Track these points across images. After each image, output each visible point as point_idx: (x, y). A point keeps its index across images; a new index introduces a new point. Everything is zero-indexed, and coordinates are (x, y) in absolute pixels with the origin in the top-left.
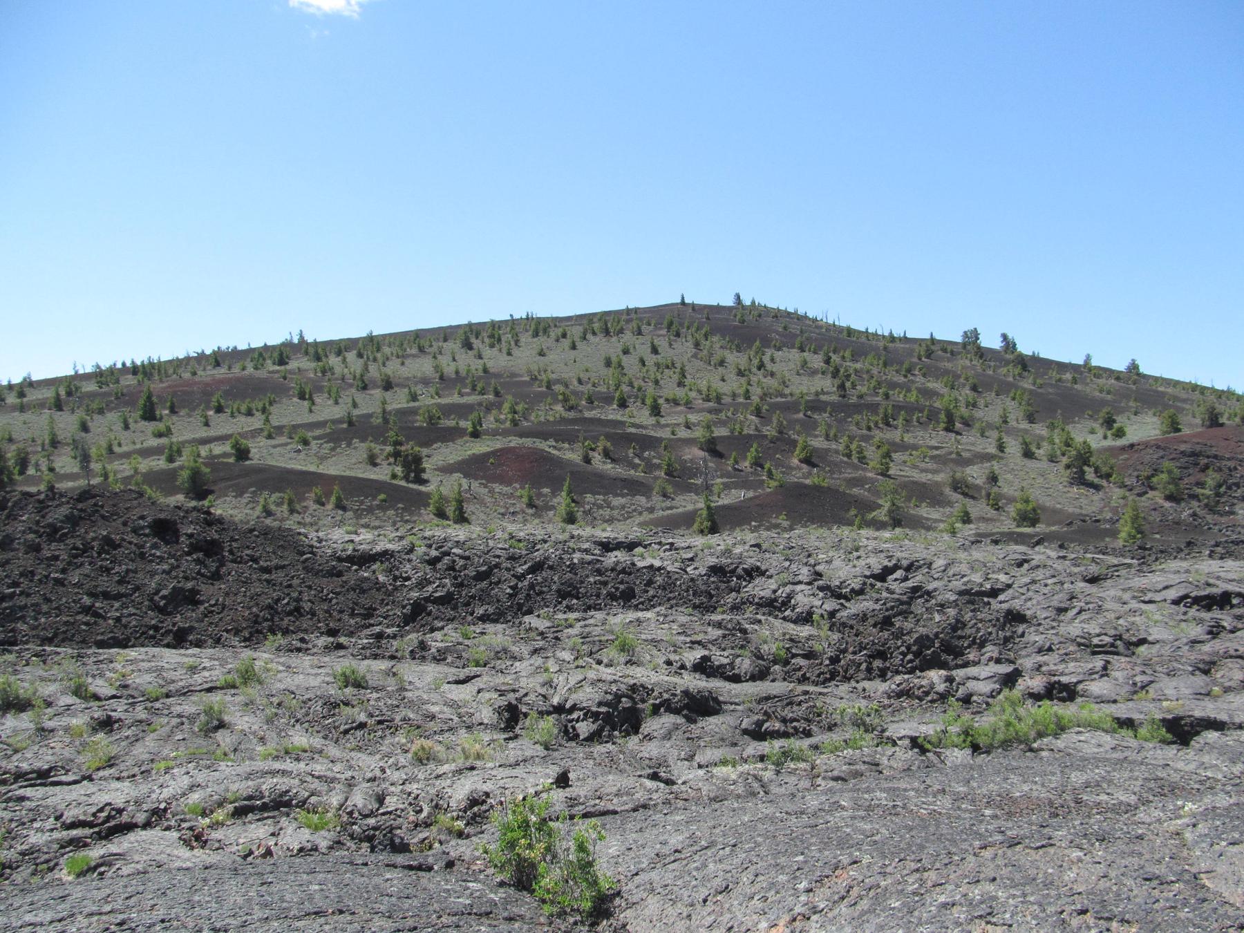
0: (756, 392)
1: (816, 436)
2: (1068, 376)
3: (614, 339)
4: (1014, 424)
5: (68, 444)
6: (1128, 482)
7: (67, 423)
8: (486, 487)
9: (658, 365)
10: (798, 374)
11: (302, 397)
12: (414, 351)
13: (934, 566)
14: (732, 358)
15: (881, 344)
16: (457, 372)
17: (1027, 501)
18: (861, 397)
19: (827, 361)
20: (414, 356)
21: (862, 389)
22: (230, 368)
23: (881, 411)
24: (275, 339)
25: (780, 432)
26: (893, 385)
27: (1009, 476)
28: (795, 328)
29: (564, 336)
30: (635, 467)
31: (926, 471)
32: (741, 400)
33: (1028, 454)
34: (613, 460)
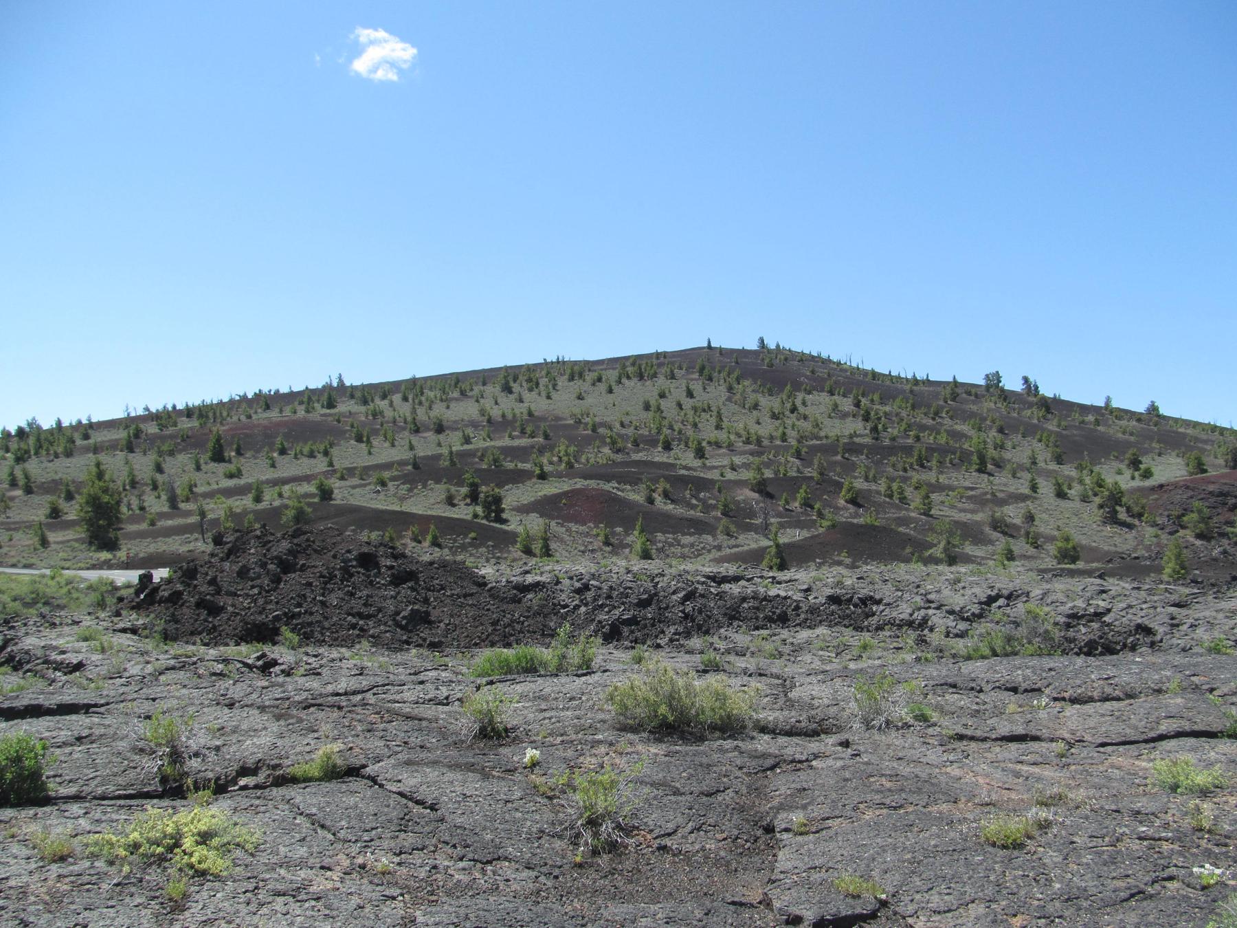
0: (792, 435)
1: (856, 478)
2: (1091, 418)
3: (648, 383)
4: (1042, 464)
5: (146, 484)
7: (143, 464)
8: (562, 526)
9: (695, 409)
10: (830, 417)
11: (359, 439)
12: (456, 394)
13: (1032, 595)
14: (765, 401)
15: (908, 387)
16: (503, 416)
17: (1067, 539)
18: (893, 439)
19: (857, 405)
20: (457, 399)
21: (893, 431)
22: (281, 411)
23: (916, 454)
24: (316, 383)
25: (821, 474)
26: (923, 428)
27: (1044, 516)
28: (822, 372)
29: (600, 380)
30: (693, 507)
31: (964, 511)
32: (778, 442)
33: (1061, 495)
34: (673, 501)
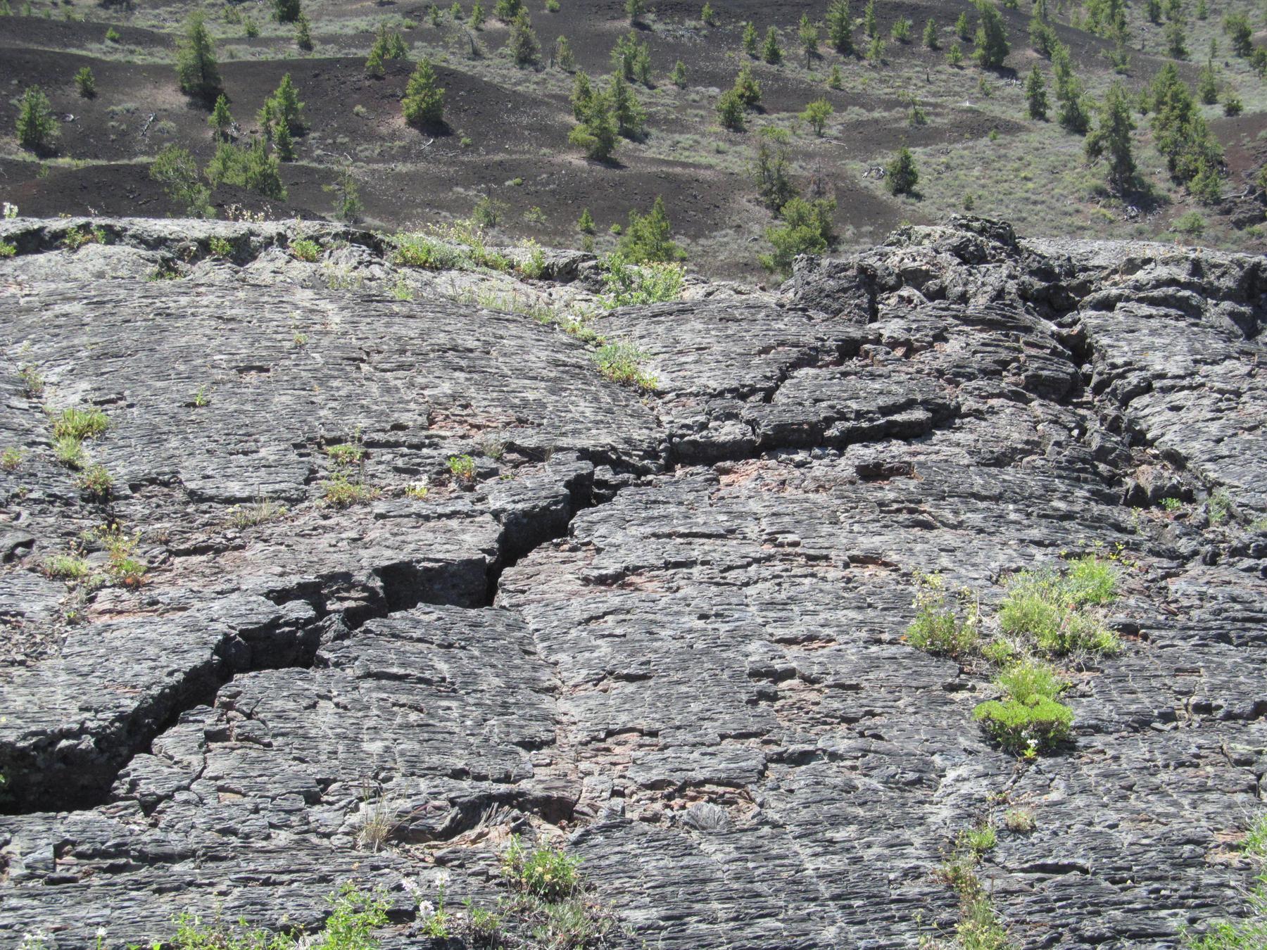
1: (607, 70)
6: (1227, 189)
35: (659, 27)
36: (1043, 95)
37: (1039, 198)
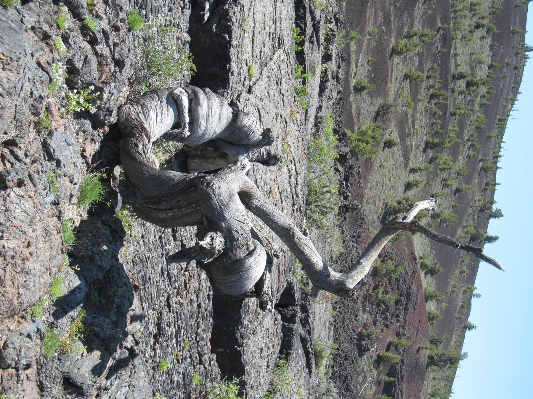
1: (423, 28)
10: (471, 54)
18: (453, 91)
26: (461, 125)
33: (408, 186)
35: (438, 37)
36: (417, 172)
37: (384, 186)
